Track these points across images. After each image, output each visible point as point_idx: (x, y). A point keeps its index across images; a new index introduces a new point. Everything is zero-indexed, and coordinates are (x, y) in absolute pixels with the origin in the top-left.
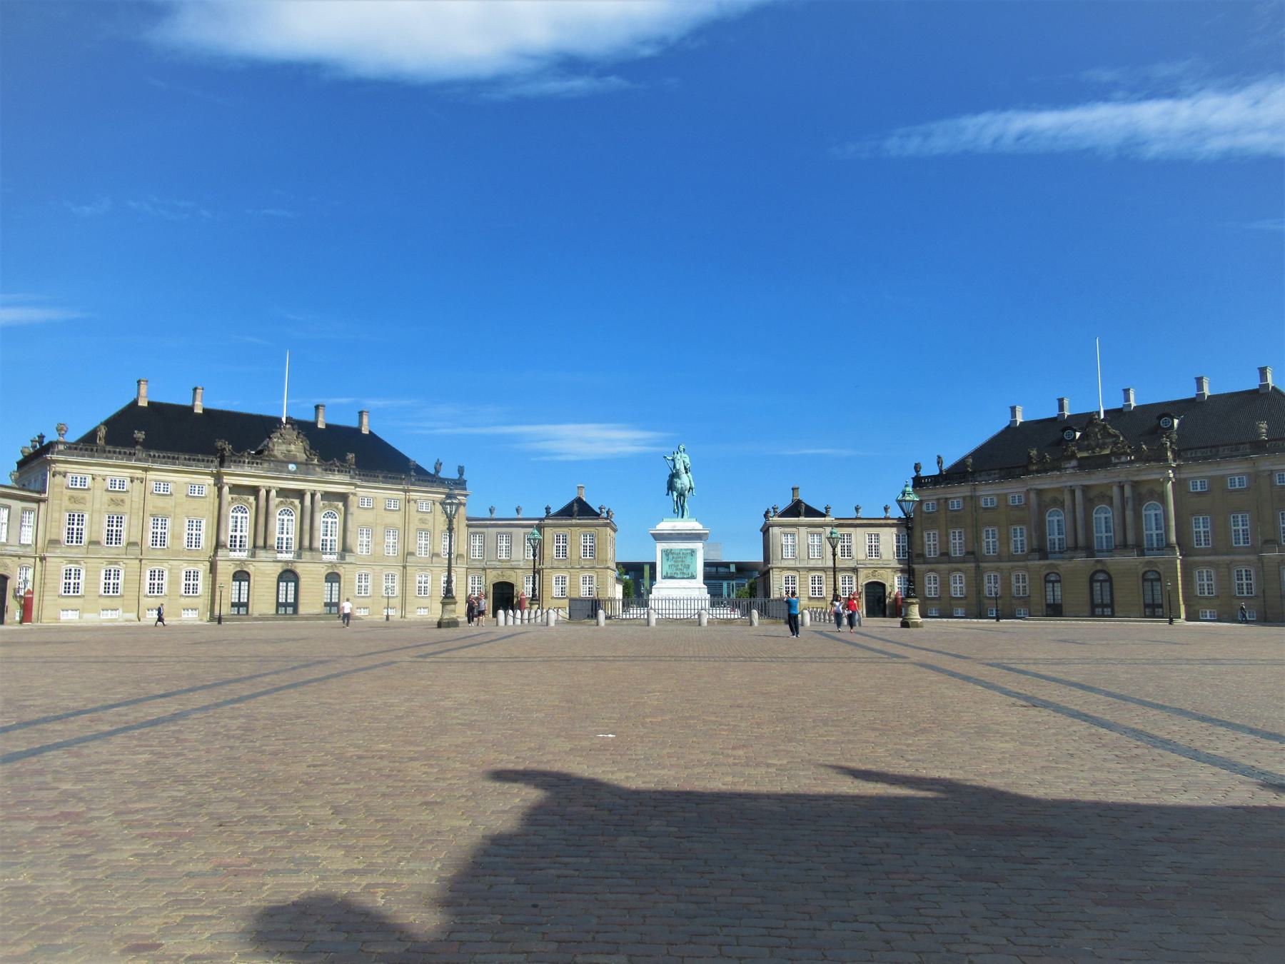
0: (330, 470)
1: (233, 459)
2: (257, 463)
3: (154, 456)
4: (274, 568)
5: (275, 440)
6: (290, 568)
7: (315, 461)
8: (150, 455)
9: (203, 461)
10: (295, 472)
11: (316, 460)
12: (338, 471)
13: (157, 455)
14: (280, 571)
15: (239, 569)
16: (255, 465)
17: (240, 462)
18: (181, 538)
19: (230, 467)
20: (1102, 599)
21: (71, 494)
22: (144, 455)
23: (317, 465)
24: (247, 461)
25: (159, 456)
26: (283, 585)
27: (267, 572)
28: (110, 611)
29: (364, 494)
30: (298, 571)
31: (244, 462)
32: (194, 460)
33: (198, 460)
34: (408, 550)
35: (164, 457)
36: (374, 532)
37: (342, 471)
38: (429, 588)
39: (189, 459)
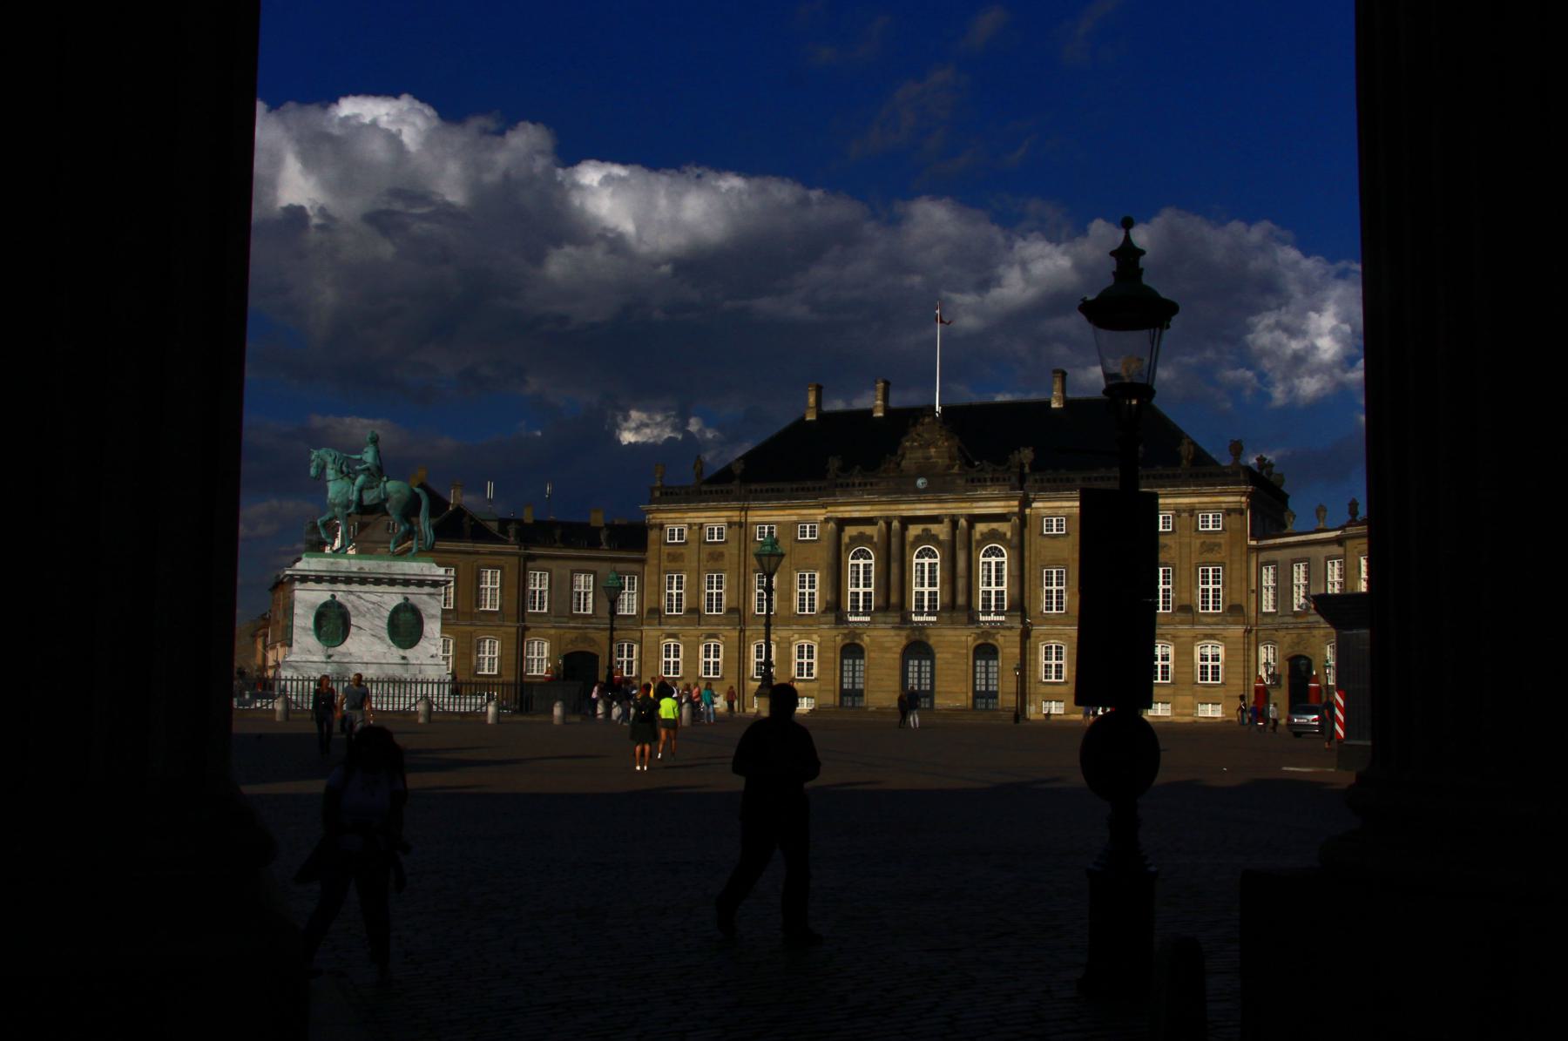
0: (979, 481)
1: (839, 481)
2: (871, 484)
3: (756, 490)
4: (897, 639)
5: (908, 444)
6: (918, 638)
7: (956, 470)
8: (751, 491)
9: (814, 489)
10: (924, 491)
11: (957, 467)
12: (992, 480)
13: (759, 488)
14: (904, 642)
15: (848, 641)
16: (869, 487)
17: (848, 485)
18: (790, 599)
19: (834, 495)
20: (987, 685)
21: (670, 551)
22: (743, 491)
23: (958, 474)
24: (857, 481)
25: (761, 491)
26: (913, 663)
27: (887, 645)
28: (1054, 703)
29: (1049, 512)
30: (931, 642)
31: (854, 485)
32: (803, 489)
33: (808, 489)
34: (1230, 601)
35: (767, 491)
36: (1177, 571)
37: (998, 480)
38: (1171, 667)
39: (797, 490)
